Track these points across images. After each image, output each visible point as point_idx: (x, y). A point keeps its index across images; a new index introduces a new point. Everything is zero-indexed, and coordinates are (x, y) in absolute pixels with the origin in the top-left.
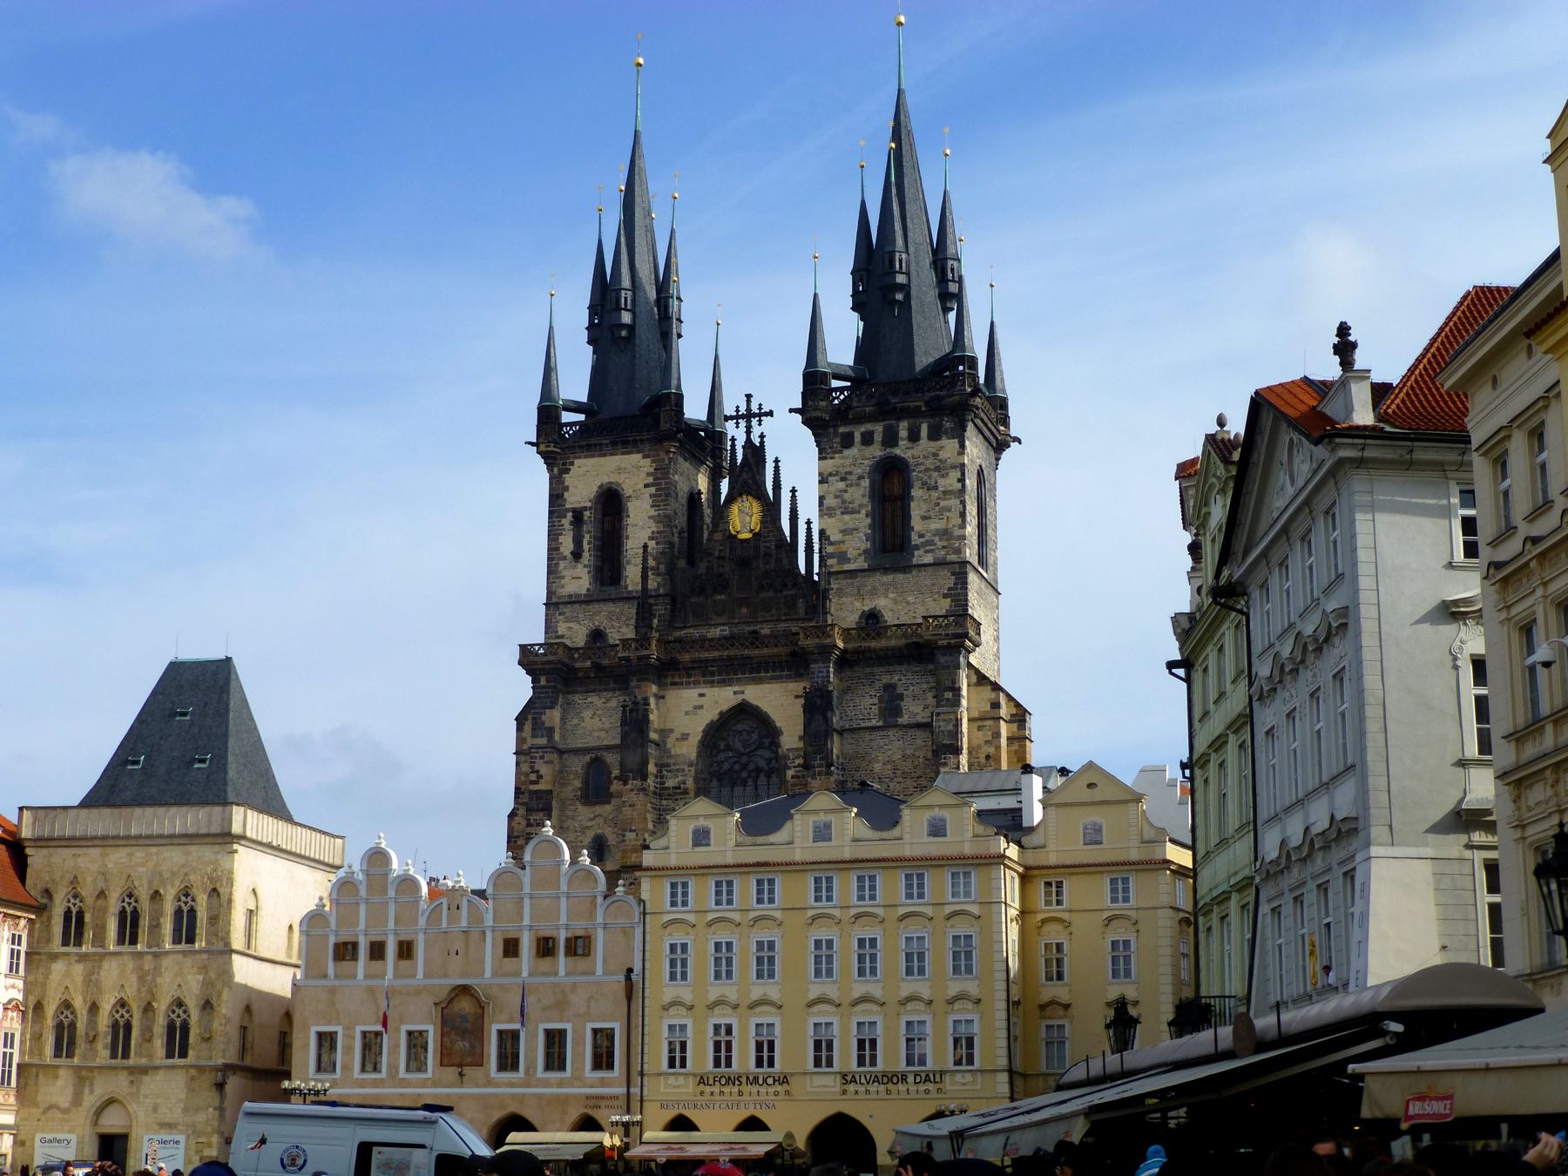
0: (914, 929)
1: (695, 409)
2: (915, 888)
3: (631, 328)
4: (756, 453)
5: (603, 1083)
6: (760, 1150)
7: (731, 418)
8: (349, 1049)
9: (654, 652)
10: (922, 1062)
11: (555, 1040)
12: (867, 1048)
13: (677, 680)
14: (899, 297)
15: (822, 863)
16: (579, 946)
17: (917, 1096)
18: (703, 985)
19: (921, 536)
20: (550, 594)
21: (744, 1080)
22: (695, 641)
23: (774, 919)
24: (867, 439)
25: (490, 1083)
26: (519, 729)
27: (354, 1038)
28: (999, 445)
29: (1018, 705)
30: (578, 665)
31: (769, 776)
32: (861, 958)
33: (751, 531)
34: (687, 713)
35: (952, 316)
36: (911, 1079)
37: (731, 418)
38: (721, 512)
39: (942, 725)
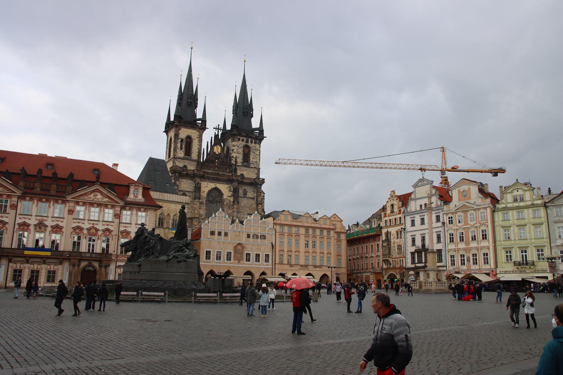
5: (267, 265)
7: (222, 130)
8: (214, 255)
11: (258, 256)
13: (202, 180)
16: (263, 237)
19: (252, 162)
20: (174, 155)
22: (206, 172)
24: (243, 140)
25: (244, 264)
27: (215, 253)
30: (182, 173)
31: (219, 203)
33: (218, 152)
34: (204, 187)
37: (222, 130)
39: (260, 199)
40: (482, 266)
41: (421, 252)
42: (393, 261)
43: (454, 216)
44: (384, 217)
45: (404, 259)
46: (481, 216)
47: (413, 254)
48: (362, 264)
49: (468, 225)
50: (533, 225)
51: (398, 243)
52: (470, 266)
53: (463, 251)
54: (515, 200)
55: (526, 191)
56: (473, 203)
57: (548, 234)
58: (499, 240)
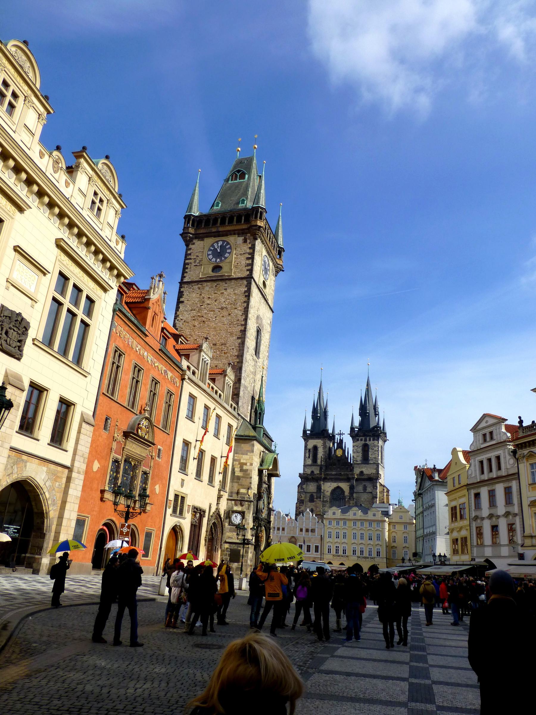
0: (370, 532)
1: (330, 431)
2: (370, 525)
3: (320, 417)
4: (341, 441)
5: (317, 555)
6: (344, 569)
9: (323, 476)
10: (371, 555)
11: (309, 547)
12: (362, 552)
14: (367, 414)
16: (313, 531)
18: (334, 539)
20: (304, 464)
24: (361, 440)
26: (298, 488)
28: (385, 441)
29: (388, 489)
32: (361, 536)
35: (377, 418)
38: (335, 451)
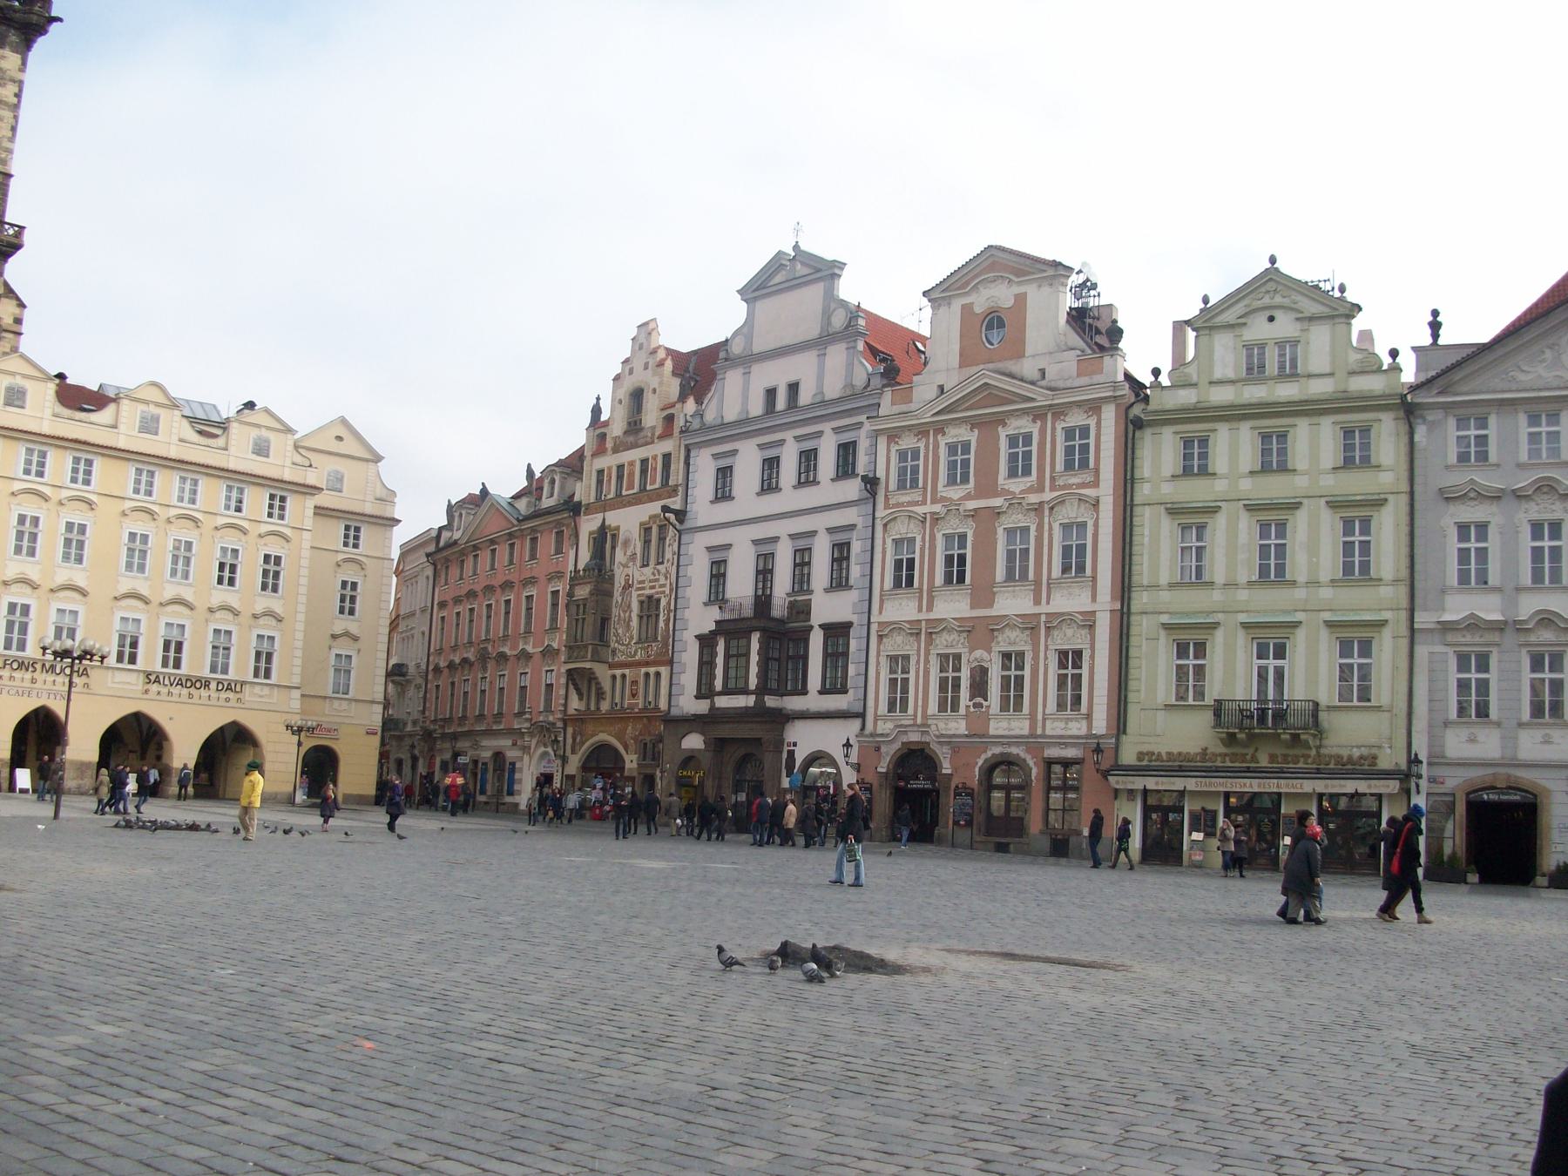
10: (225, 671)
12: (173, 650)
15: (132, 452)
17: (209, 703)
21: (38, 666)
23: (90, 503)
36: (213, 685)
40: (1044, 720)
41: (746, 634)
42: (614, 677)
43: (927, 447)
44: (594, 455)
45: (664, 671)
46: (1069, 451)
47: (706, 642)
48: (483, 692)
49: (996, 494)
50: (1333, 505)
51: (647, 585)
52: (986, 718)
53: (954, 636)
54: (1255, 371)
55: (1311, 319)
56: (1036, 375)
57: (1404, 562)
58: (1145, 583)
